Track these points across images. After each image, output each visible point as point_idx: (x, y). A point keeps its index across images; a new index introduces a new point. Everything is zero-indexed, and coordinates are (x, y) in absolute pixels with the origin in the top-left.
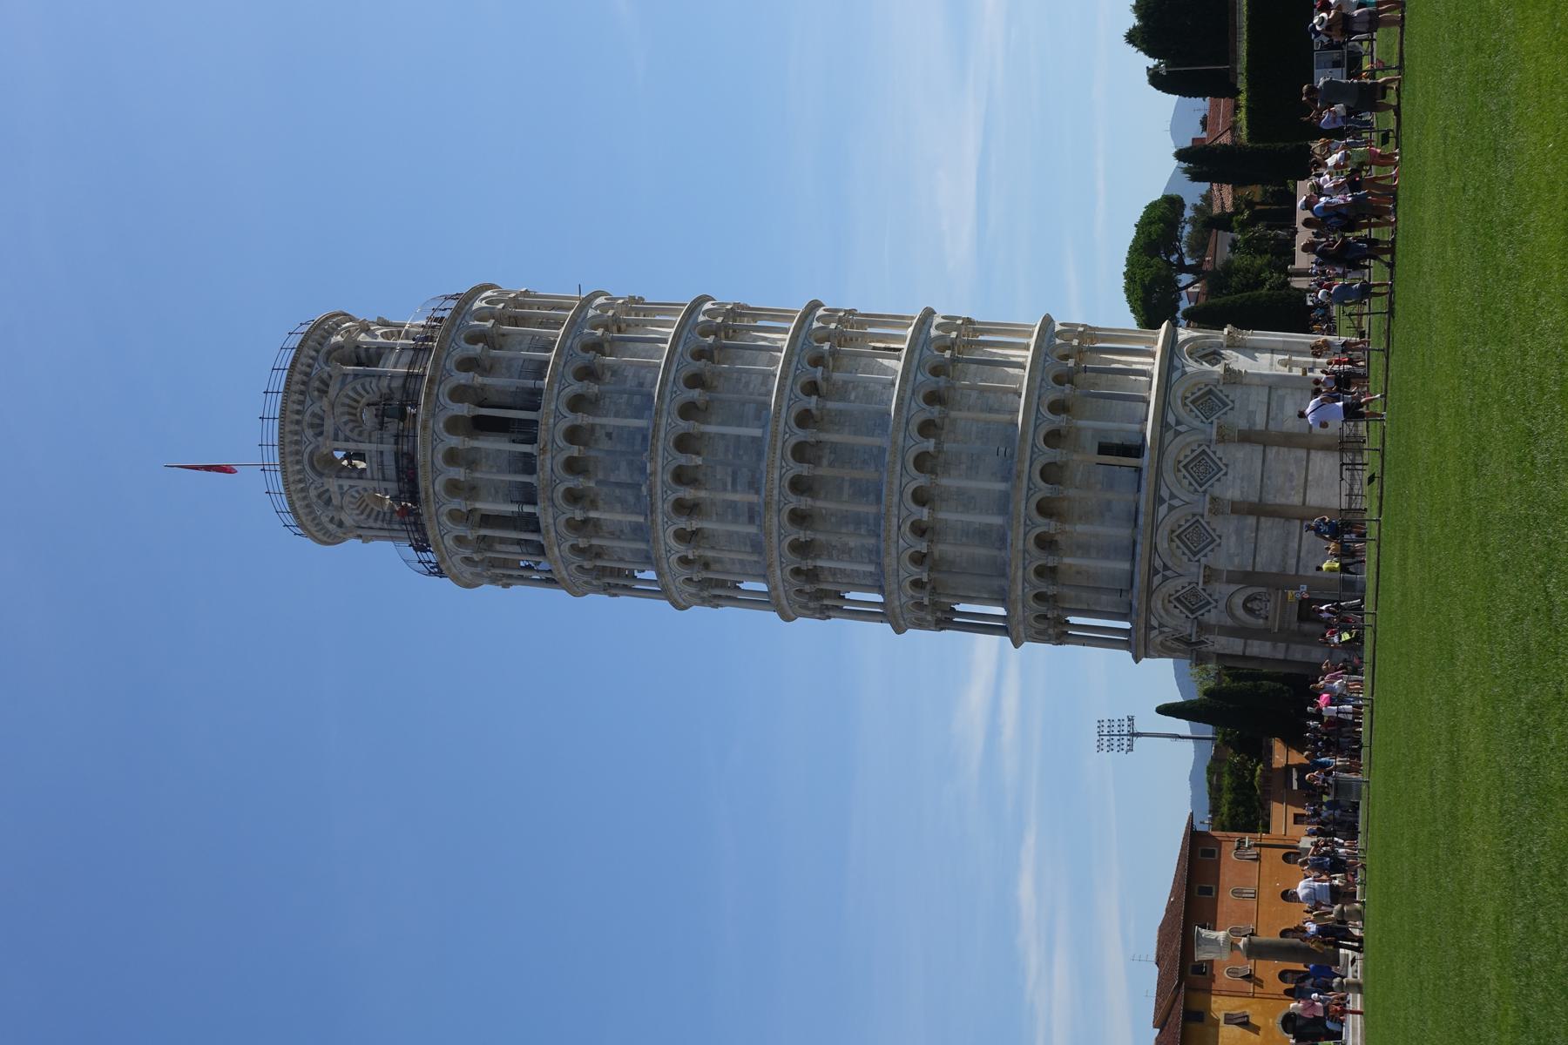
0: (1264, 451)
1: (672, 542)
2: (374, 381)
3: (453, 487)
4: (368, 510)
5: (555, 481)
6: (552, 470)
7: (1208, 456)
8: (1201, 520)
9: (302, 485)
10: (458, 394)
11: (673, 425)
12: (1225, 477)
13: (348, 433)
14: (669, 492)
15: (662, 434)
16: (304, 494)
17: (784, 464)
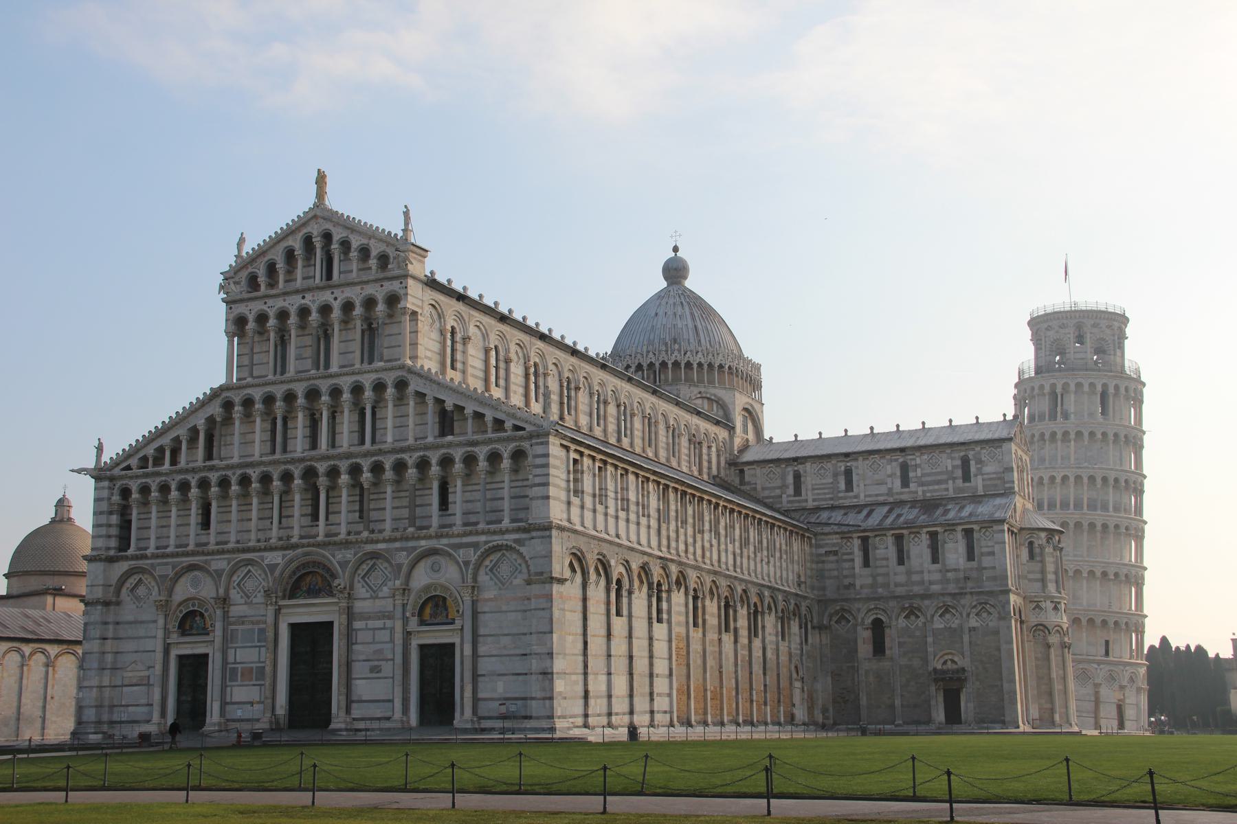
1: (1063, 474)
3: (1079, 385)
10: (1117, 387)
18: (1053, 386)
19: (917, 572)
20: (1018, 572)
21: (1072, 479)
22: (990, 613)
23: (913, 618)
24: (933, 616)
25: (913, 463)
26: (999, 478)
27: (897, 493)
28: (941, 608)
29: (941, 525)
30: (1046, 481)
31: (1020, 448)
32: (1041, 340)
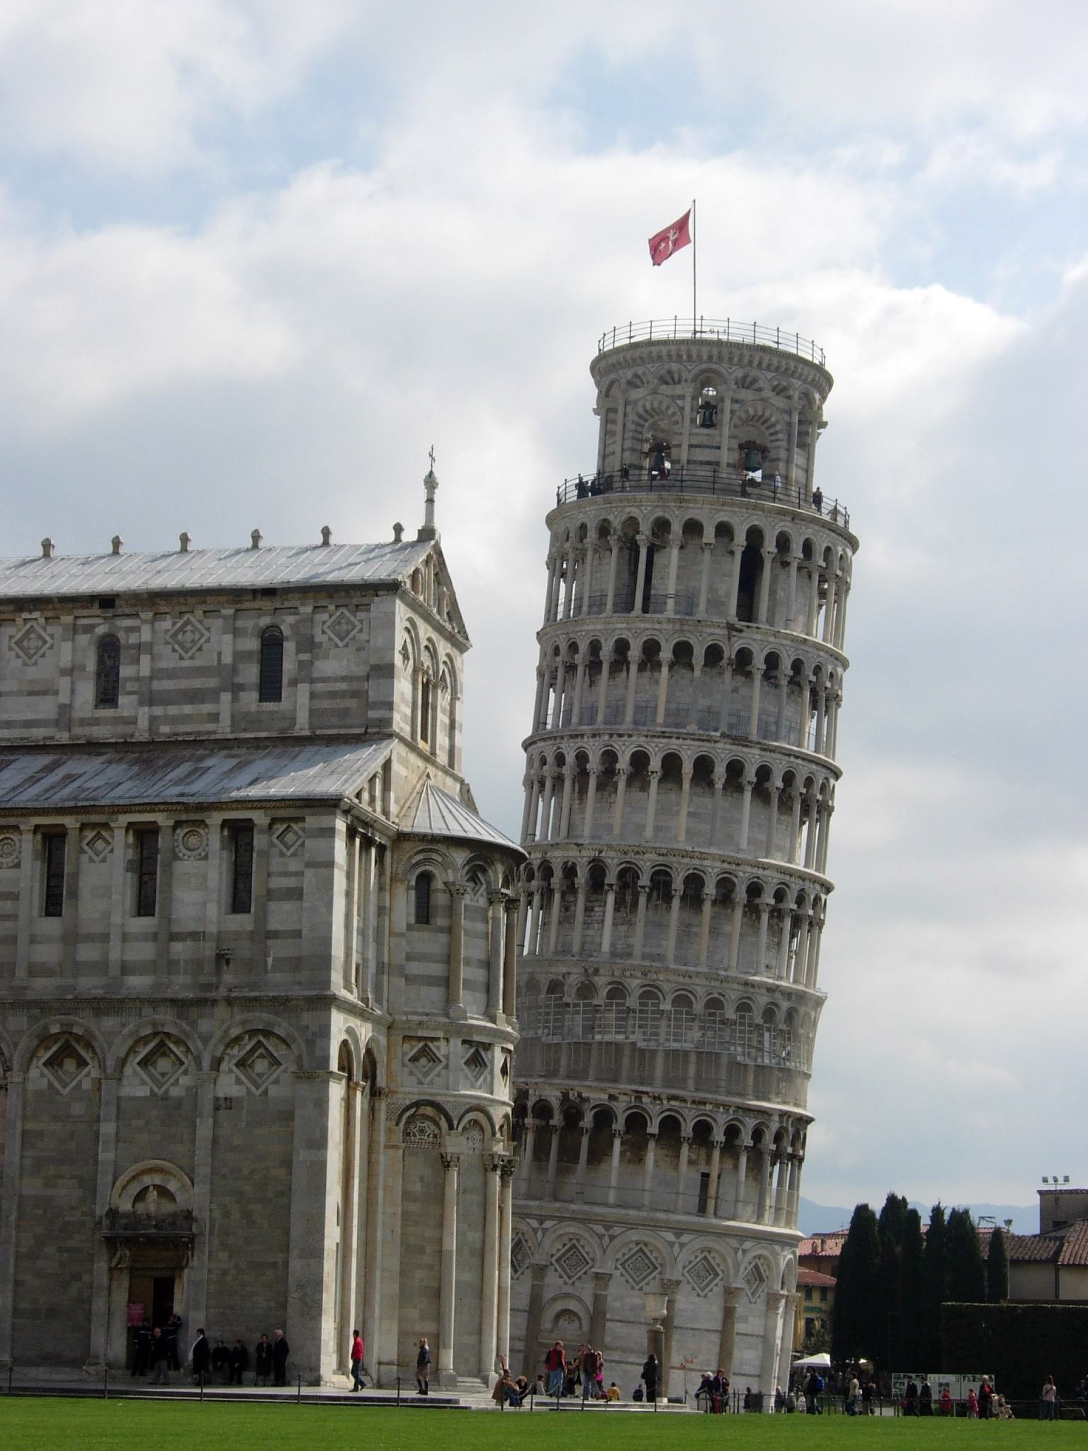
0: (715, 1331)
2: (784, 444)
4: (648, 417)
5: (701, 636)
6: (712, 634)
7: (713, 1279)
8: (657, 1271)
9: (685, 357)
10: (783, 542)
11: (753, 760)
12: (695, 1295)
13: (737, 414)
14: (689, 752)
15: (745, 750)
16: (675, 357)
17: (716, 870)
18: (632, 523)
19: (91, 938)
20: (379, 952)
21: (655, 764)
22: (275, 1062)
23: (70, 1065)
24: (123, 1062)
25: (133, 639)
26: (355, 694)
27: (83, 722)
28: (144, 1040)
29: (165, 806)
30: (594, 765)
31: (428, 618)
32: (616, 411)
